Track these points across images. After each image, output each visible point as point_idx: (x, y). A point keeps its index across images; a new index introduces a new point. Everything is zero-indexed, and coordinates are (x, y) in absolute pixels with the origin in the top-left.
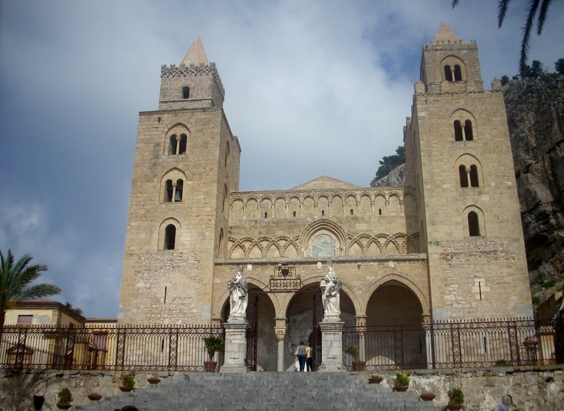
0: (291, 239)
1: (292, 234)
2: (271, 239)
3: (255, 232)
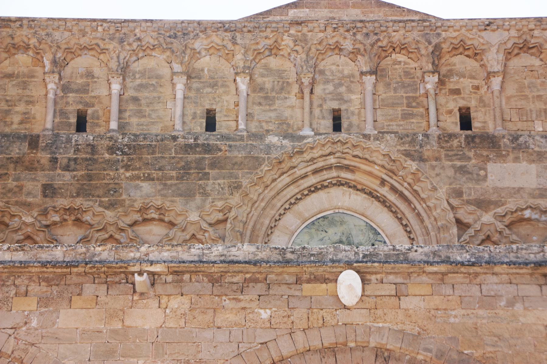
0: (194, 217)
1: (198, 199)
2: (101, 214)
3: (29, 185)
